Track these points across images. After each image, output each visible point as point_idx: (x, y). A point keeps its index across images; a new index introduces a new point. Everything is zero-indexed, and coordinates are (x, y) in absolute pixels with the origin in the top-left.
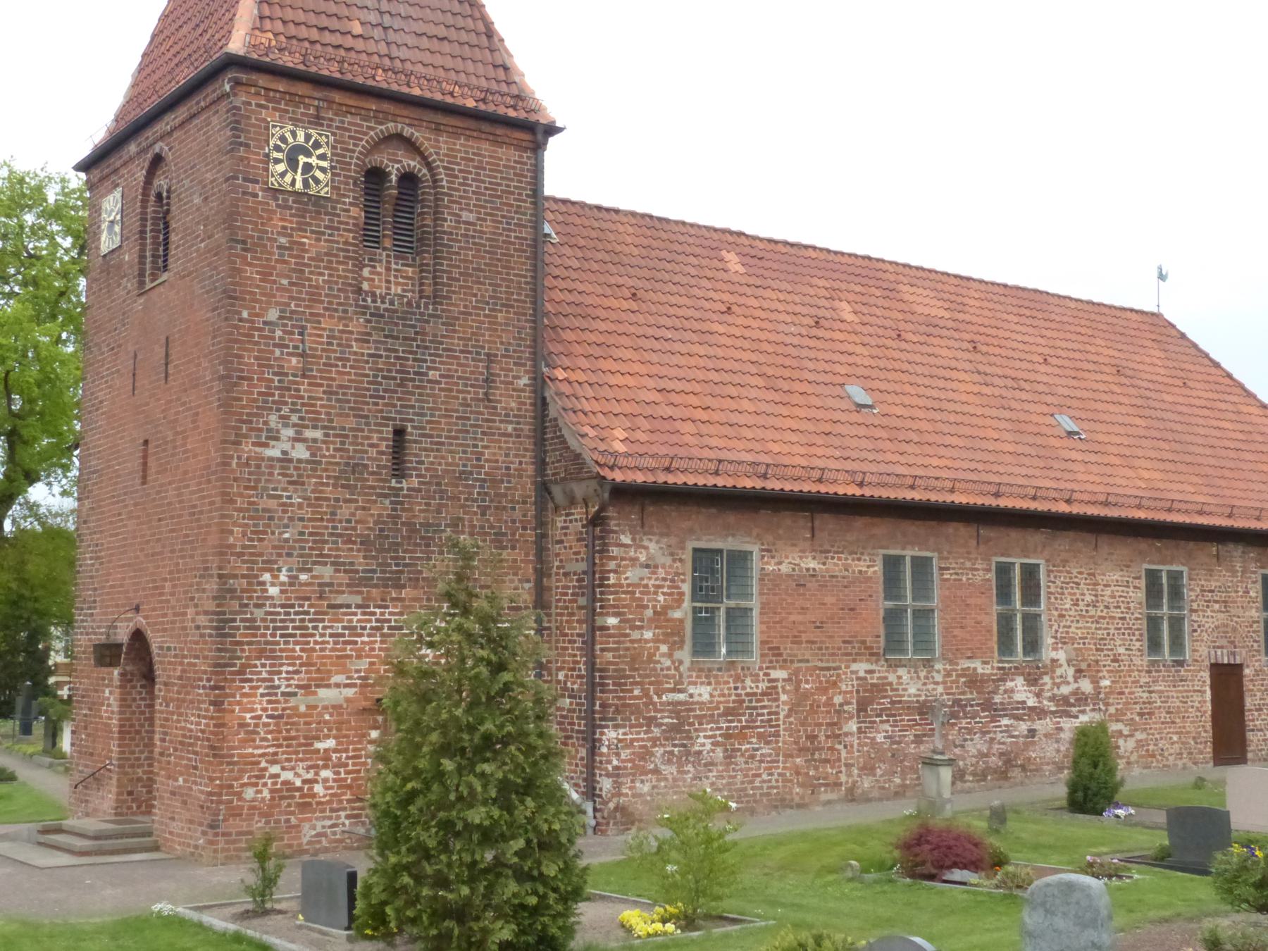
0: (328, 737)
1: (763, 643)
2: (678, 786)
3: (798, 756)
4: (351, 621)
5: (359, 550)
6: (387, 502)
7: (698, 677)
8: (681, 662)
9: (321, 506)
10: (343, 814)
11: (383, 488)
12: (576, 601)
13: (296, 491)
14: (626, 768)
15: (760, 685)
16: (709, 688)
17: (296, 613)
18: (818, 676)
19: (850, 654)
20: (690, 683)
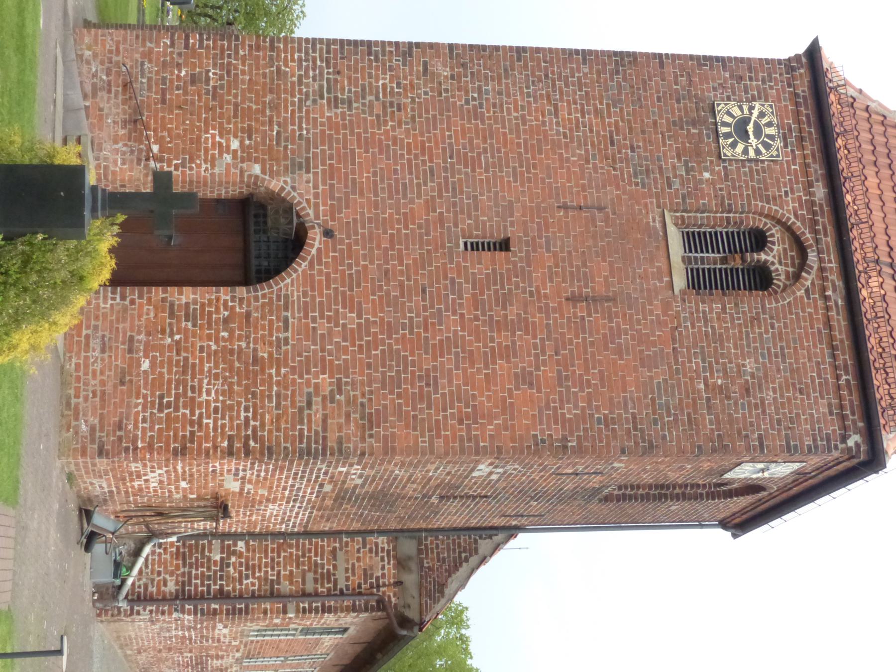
12: (310, 570)
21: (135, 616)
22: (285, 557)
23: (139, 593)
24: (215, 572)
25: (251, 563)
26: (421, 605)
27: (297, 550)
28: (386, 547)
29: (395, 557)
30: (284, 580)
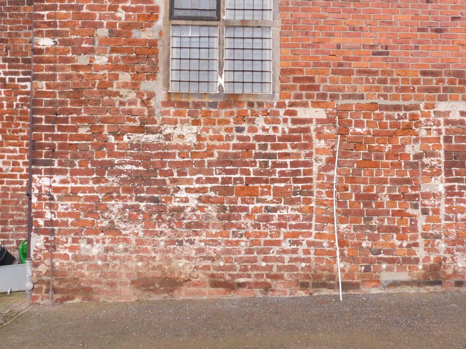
1: (283, 72)
2: (146, 250)
3: (341, 221)
7: (177, 113)
8: (151, 95)
14: (65, 224)
15: (280, 127)
16: (195, 128)
18: (379, 117)
19: (437, 90)
20: (164, 122)
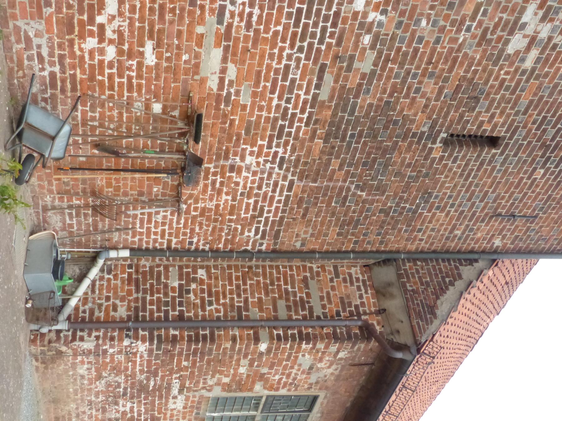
0: (159, 57)
4: (300, 87)
5: (380, 99)
6: (425, 129)
9: (445, 63)
10: (57, 69)
11: (442, 125)
12: (280, 297)
13: (474, 37)
17: (324, 29)
21: (77, 343)
22: (251, 285)
23: (83, 319)
24: (174, 298)
25: (214, 290)
26: (412, 327)
27: (265, 277)
28: (361, 278)
29: (372, 287)
30: (253, 307)
